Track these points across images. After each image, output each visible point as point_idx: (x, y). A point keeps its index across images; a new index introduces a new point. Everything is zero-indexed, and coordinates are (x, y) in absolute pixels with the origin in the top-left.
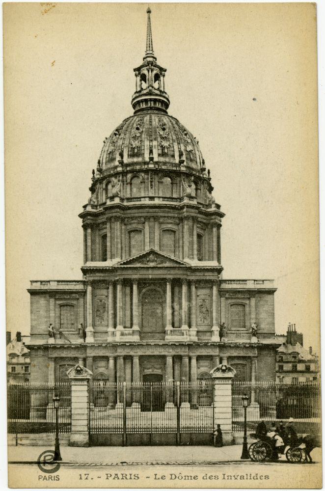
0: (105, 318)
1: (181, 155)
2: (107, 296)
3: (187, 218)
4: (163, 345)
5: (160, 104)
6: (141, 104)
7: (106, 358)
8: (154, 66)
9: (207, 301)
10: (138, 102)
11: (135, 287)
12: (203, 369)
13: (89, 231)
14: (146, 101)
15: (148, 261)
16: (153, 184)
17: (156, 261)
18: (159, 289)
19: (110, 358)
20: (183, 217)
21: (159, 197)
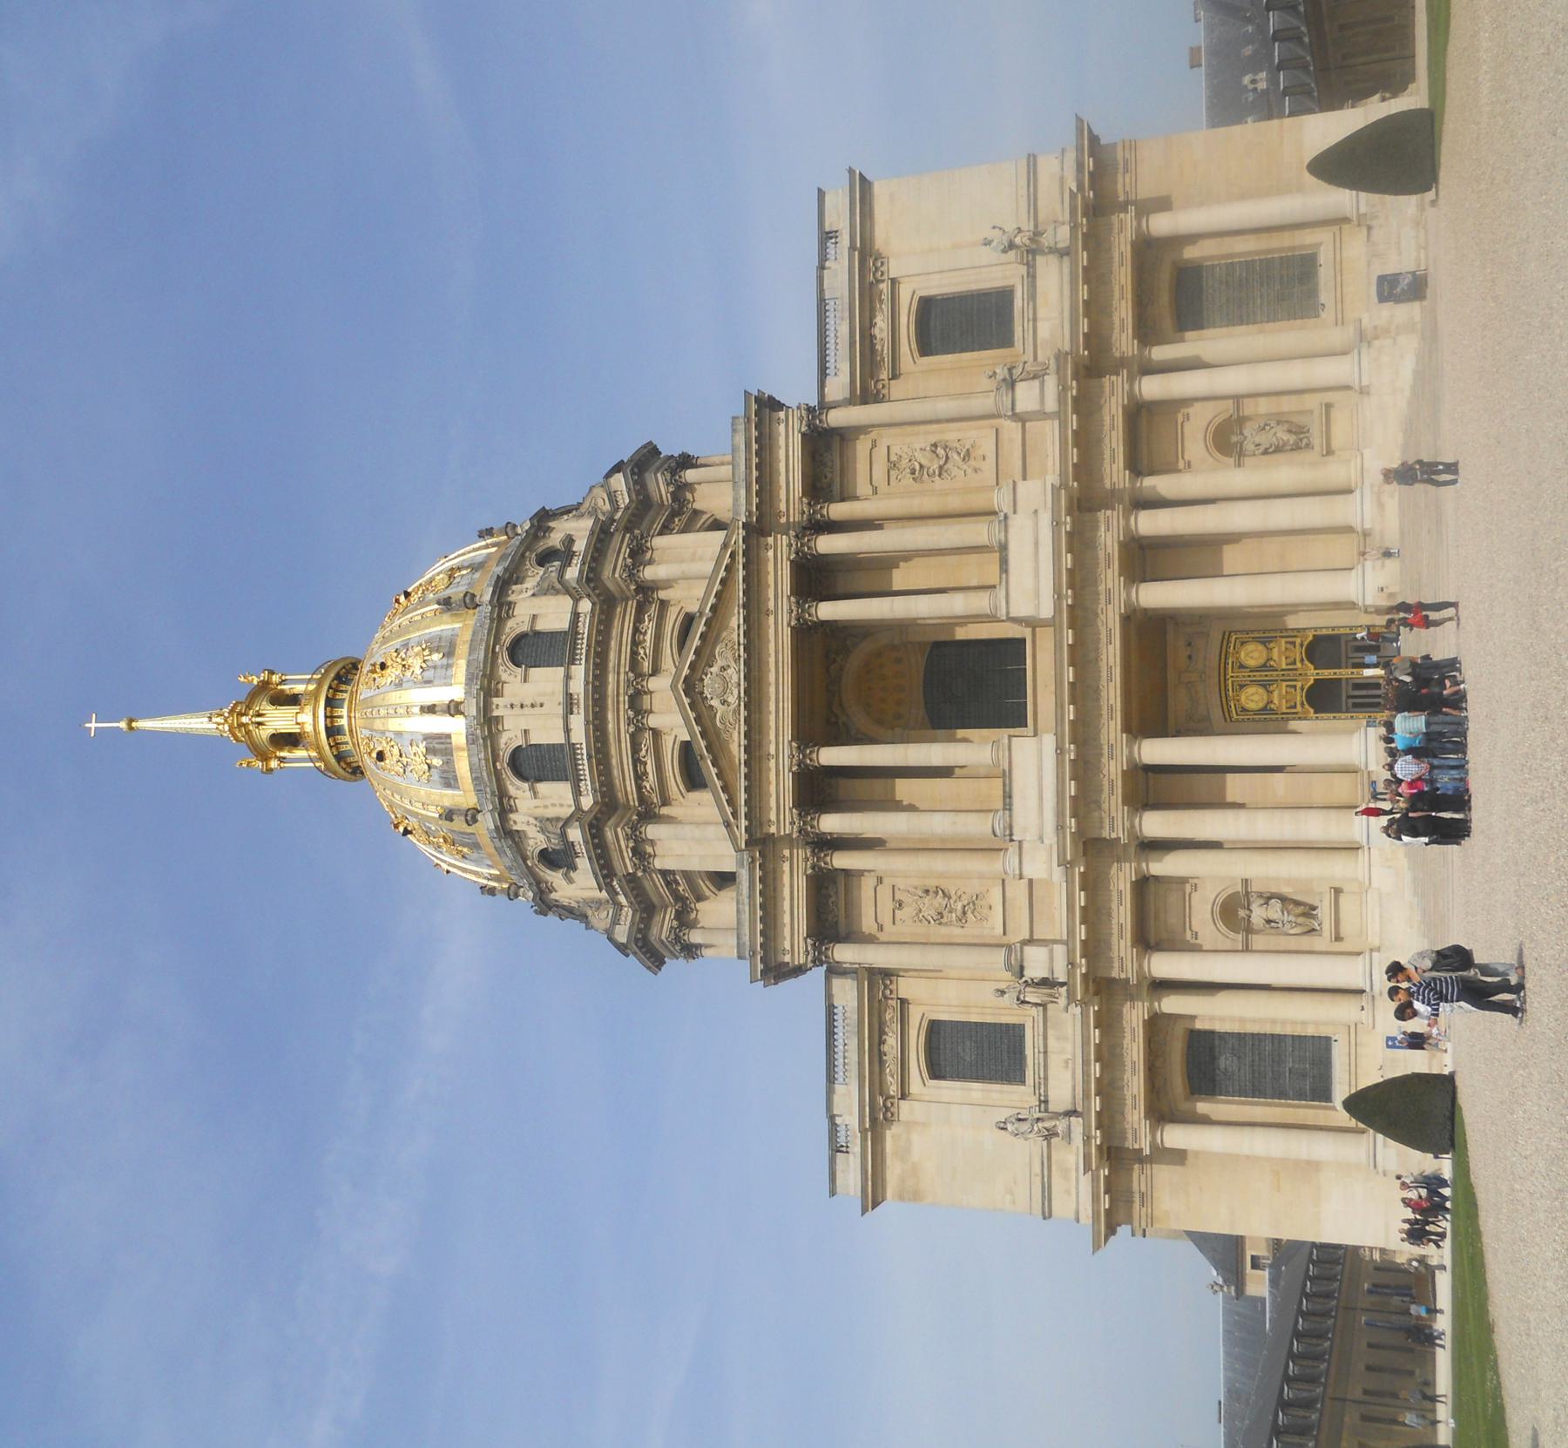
0: (973, 887)
2: (880, 880)
4: (1071, 626)
5: (343, 687)
6: (343, 748)
7: (1143, 886)
8: (249, 707)
10: (340, 757)
11: (831, 756)
13: (695, 937)
14: (332, 731)
15: (724, 702)
16: (527, 702)
17: (723, 669)
18: (855, 661)
21: (568, 677)
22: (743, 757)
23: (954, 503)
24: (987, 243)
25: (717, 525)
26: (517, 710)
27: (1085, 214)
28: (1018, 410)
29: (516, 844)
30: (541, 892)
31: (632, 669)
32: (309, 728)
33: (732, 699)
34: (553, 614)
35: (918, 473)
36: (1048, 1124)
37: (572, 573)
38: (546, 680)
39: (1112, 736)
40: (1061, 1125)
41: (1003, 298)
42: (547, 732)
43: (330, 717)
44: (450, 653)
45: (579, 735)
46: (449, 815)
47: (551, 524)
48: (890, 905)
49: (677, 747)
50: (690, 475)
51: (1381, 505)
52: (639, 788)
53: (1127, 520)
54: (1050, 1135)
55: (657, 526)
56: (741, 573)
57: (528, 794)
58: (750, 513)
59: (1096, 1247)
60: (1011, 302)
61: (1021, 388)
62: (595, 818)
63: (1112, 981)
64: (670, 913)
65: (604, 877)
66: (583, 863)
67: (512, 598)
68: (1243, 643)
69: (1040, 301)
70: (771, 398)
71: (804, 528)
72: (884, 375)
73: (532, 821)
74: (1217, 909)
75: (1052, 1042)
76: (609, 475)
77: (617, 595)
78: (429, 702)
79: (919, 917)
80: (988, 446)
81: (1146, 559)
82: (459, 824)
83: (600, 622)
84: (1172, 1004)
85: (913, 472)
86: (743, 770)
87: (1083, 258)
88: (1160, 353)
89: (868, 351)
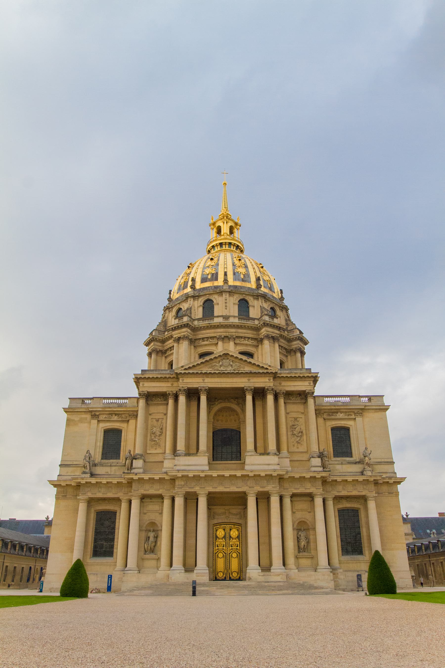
1: (258, 279)
3: (267, 337)
4: (243, 476)
5: (235, 248)
6: (216, 248)
7: (161, 497)
9: (301, 420)
10: (213, 247)
11: (203, 399)
12: (299, 515)
13: (153, 356)
14: (221, 244)
16: (227, 304)
17: (231, 366)
18: (234, 406)
19: (165, 498)
20: (262, 337)
21: (234, 317)
22: (203, 372)
23: (284, 438)
24: (366, 449)
25: (282, 364)
26: (224, 301)
27: (374, 480)
28: (312, 459)
29: (184, 301)
30: (169, 309)
31: (236, 337)
32: (223, 237)
33: (222, 368)
34: (254, 312)
35: (293, 427)
36: (88, 466)
37: (267, 318)
38: (234, 310)
39: (207, 488)
40: (88, 470)
41: (350, 454)
42: (217, 311)
43: (226, 244)
44: (243, 280)
45: (217, 321)
46: (193, 280)
47: (284, 311)
48: (157, 417)
49: (212, 351)
50: (299, 355)
51: (279, 575)
52: (200, 339)
53: (276, 494)
54: (85, 467)
55: (282, 345)
56: (261, 371)
57: (199, 304)
58: (280, 374)
59: (50, 481)
60: (347, 457)
61: (320, 459)
62: (190, 325)
63: (131, 487)
64: (161, 348)
65: (172, 328)
66: (177, 321)
67: (260, 300)
68: (238, 530)
69: (348, 466)
70: (318, 380)
71: (276, 391)
72: (325, 416)
73: (191, 306)
74: (153, 521)
75: (114, 468)
76: (298, 329)
77: (260, 332)
78: (228, 274)
79: (153, 426)
80: (301, 450)
81: (263, 498)
82: (190, 283)
83: (251, 327)
84: (124, 505)
85: (293, 426)
86: (199, 372)
87: (361, 478)
88: (330, 503)
89: (333, 411)
